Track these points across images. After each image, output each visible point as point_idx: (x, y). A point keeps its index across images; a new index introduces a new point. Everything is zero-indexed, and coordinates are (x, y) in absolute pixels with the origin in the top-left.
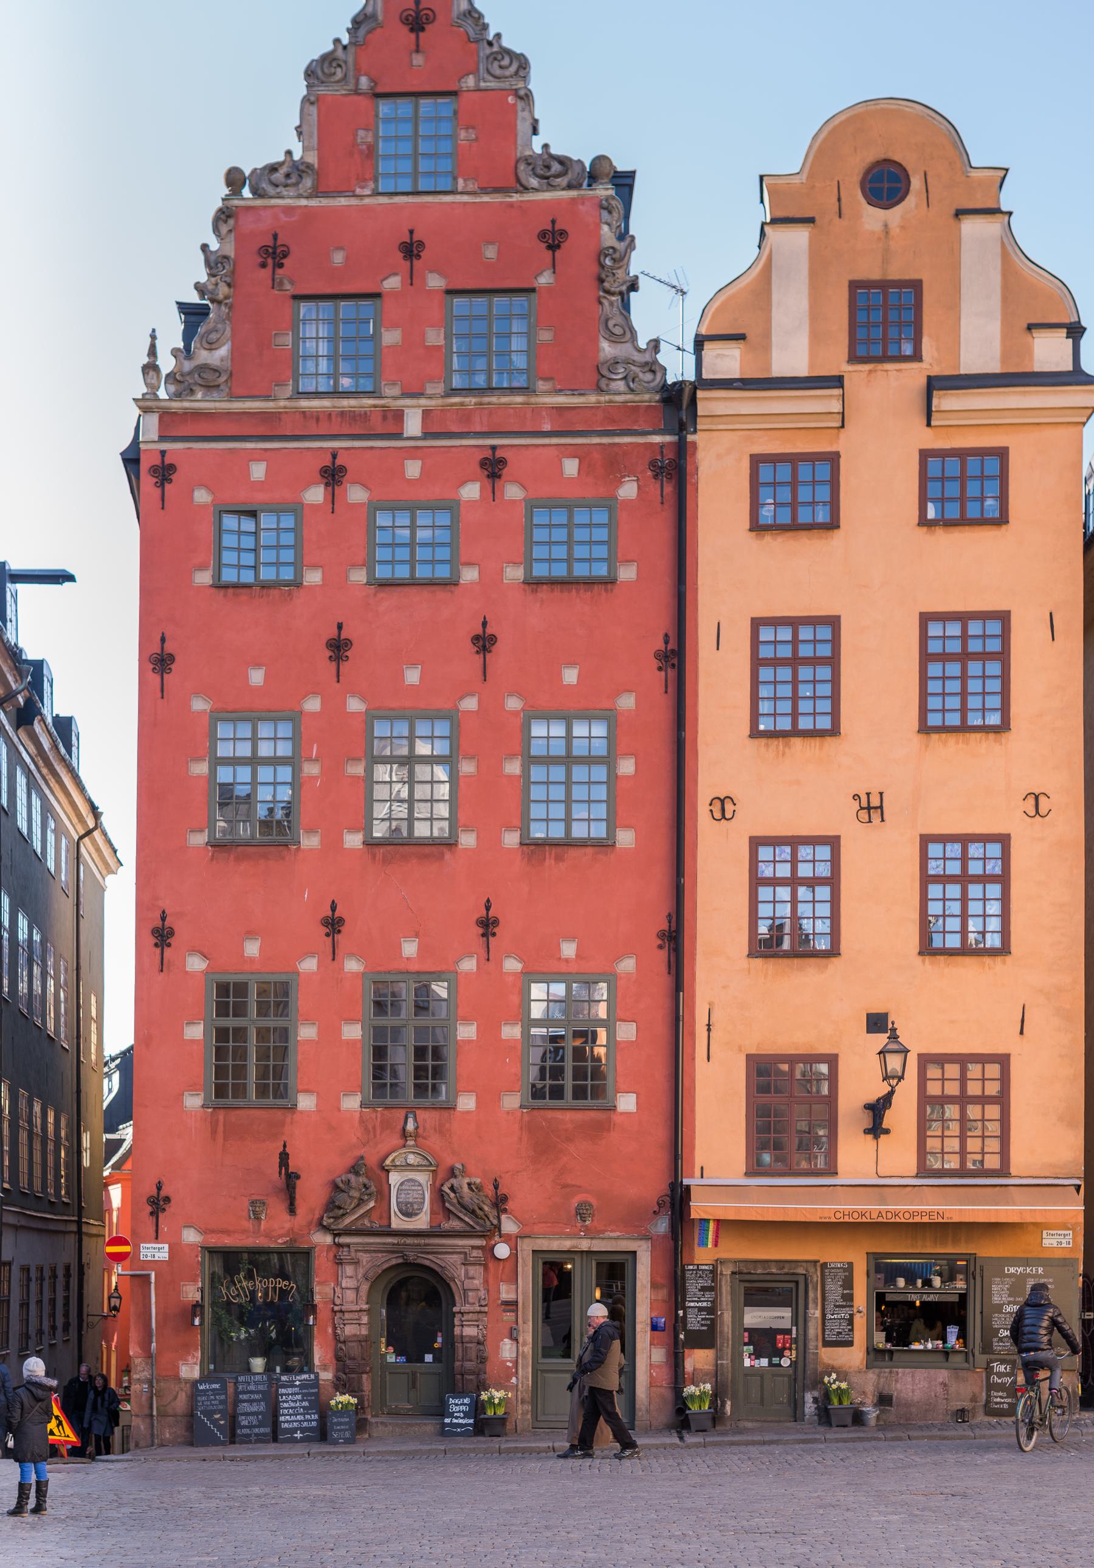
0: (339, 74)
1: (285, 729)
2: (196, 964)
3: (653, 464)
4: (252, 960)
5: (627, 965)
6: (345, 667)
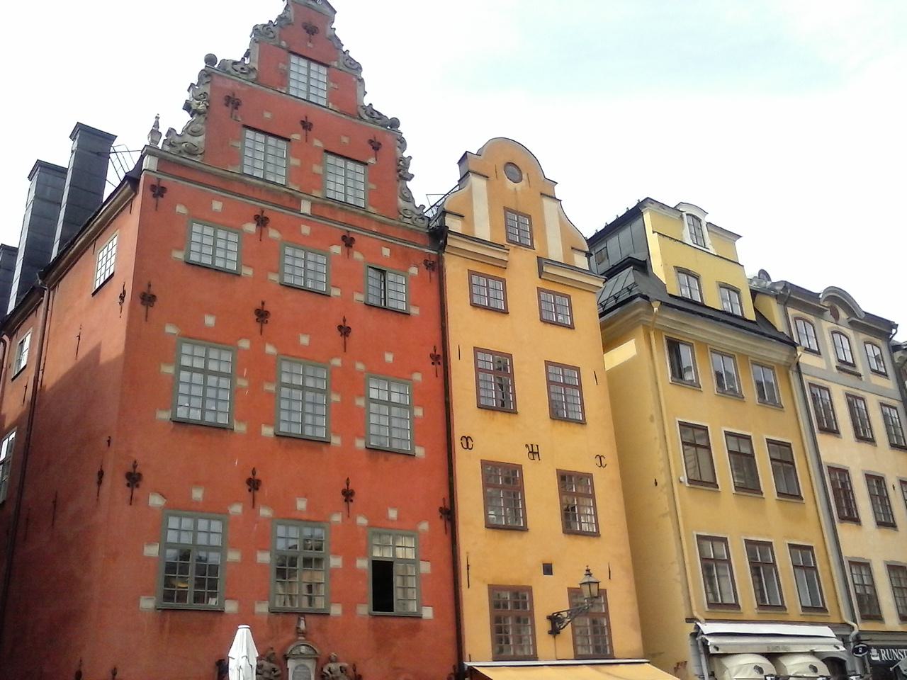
0: (271, 35)
1: (227, 356)
2: (156, 501)
3: (426, 261)
4: (197, 503)
5: (424, 526)
6: (265, 327)
